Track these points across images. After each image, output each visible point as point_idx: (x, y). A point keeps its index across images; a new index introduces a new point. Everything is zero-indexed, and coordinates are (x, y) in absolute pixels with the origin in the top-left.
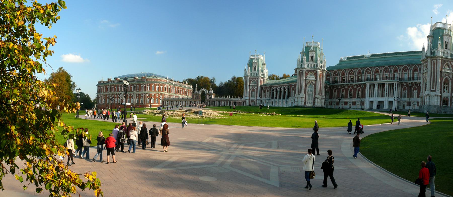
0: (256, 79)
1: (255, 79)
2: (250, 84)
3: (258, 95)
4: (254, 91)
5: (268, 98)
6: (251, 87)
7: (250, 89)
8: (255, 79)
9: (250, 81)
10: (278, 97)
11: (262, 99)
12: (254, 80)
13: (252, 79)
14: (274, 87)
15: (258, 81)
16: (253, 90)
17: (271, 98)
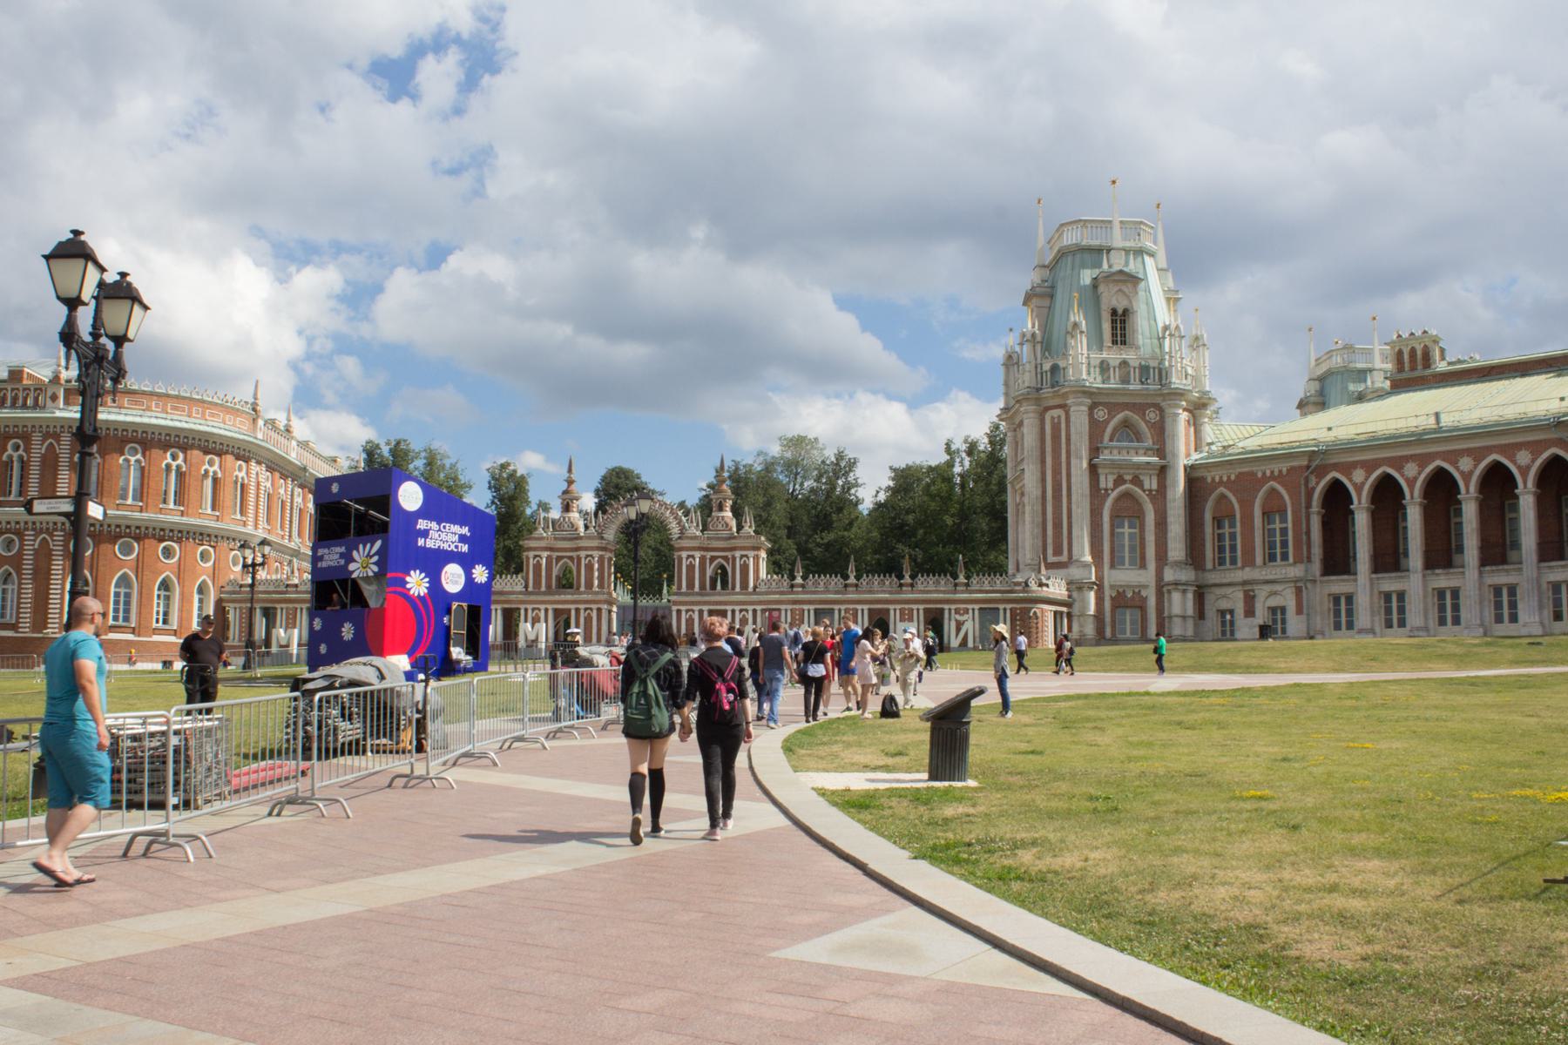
0: (1144, 405)
1: (1140, 409)
2: (1095, 451)
3: (1177, 548)
4: (1139, 516)
5: (1296, 571)
6: (1106, 481)
7: (1097, 494)
8: (1140, 409)
9: (1096, 428)
10: (1415, 558)
11: (1213, 578)
12: (1126, 424)
13: (1113, 408)
14: (1347, 468)
15: (1161, 431)
16: (1128, 509)
17: (1316, 567)
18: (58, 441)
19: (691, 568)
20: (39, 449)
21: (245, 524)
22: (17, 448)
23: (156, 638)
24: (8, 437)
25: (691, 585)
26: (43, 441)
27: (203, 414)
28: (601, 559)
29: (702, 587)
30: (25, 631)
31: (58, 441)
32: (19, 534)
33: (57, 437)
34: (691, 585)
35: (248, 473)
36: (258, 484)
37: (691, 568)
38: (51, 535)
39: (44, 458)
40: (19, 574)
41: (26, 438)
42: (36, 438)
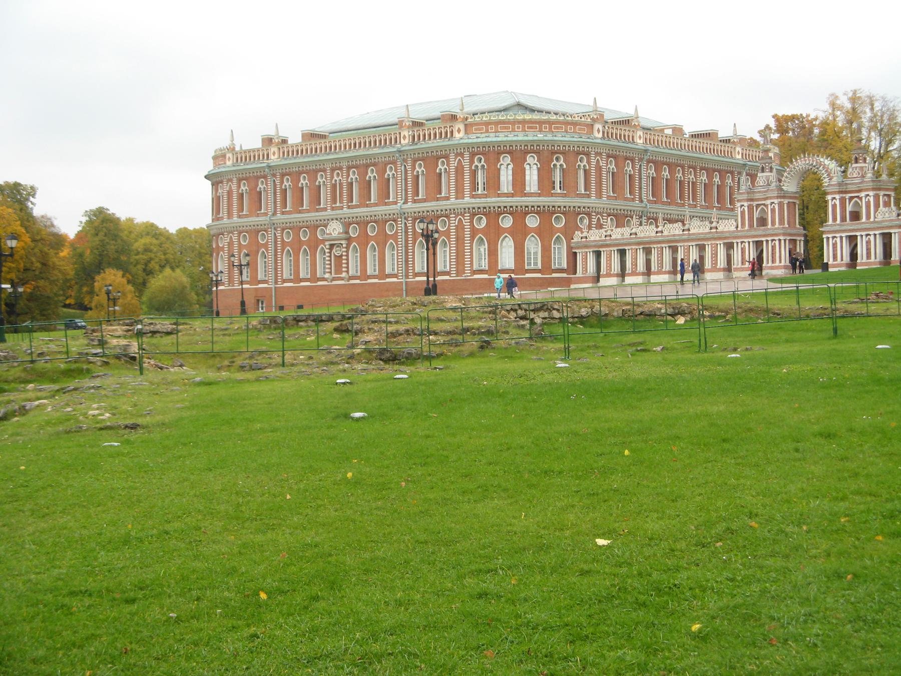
18: (463, 157)
19: (834, 206)
20: (454, 164)
21: (589, 196)
22: (443, 163)
23: (528, 275)
24: (438, 158)
25: (835, 219)
26: (455, 159)
27: (550, 128)
28: (781, 205)
29: (843, 219)
30: (453, 277)
31: (463, 157)
32: (447, 216)
33: (462, 155)
34: (835, 219)
35: (589, 162)
36: (599, 169)
37: (834, 206)
38: (464, 216)
39: (457, 168)
40: (450, 242)
41: (446, 157)
42: (452, 156)
